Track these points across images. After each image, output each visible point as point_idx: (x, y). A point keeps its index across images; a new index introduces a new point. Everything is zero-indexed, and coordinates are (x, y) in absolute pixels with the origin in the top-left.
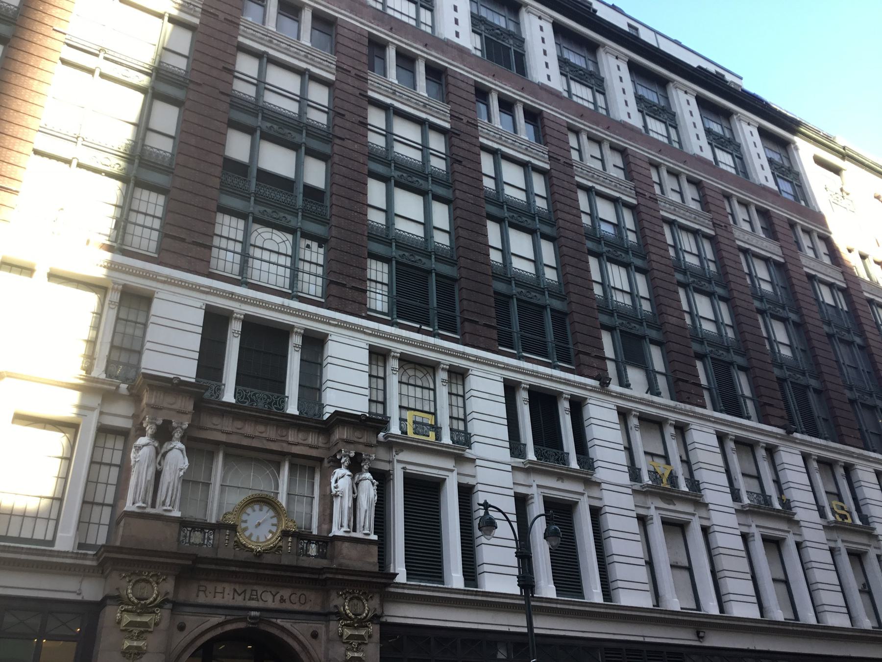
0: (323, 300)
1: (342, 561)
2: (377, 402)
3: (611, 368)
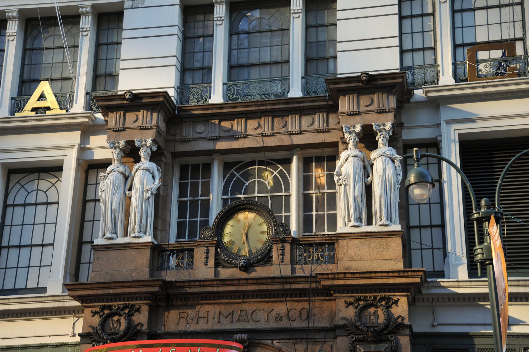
1: (349, 264)
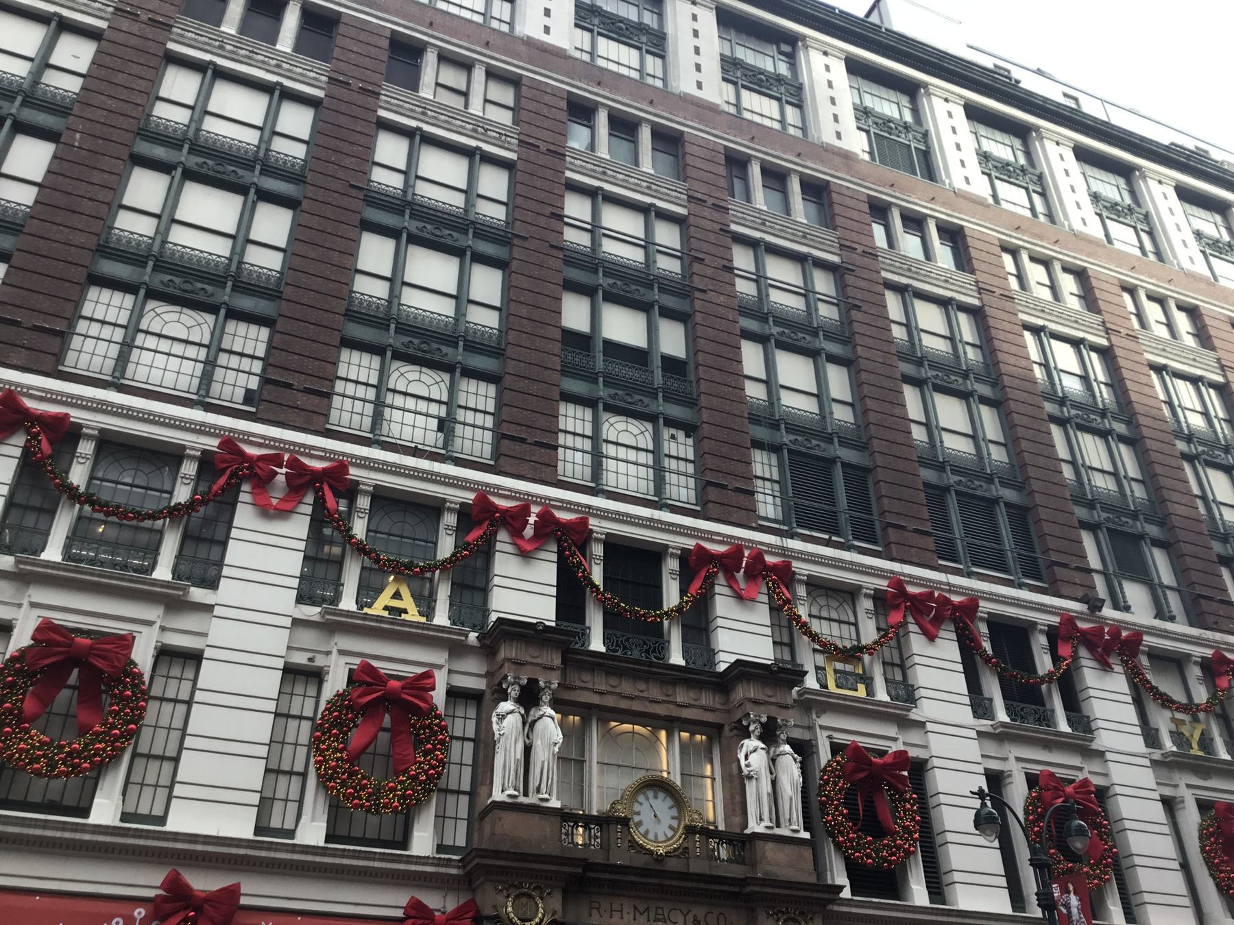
0: (698, 508)
1: (767, 868)
2: (893, 665)
3: (1099, 581)
